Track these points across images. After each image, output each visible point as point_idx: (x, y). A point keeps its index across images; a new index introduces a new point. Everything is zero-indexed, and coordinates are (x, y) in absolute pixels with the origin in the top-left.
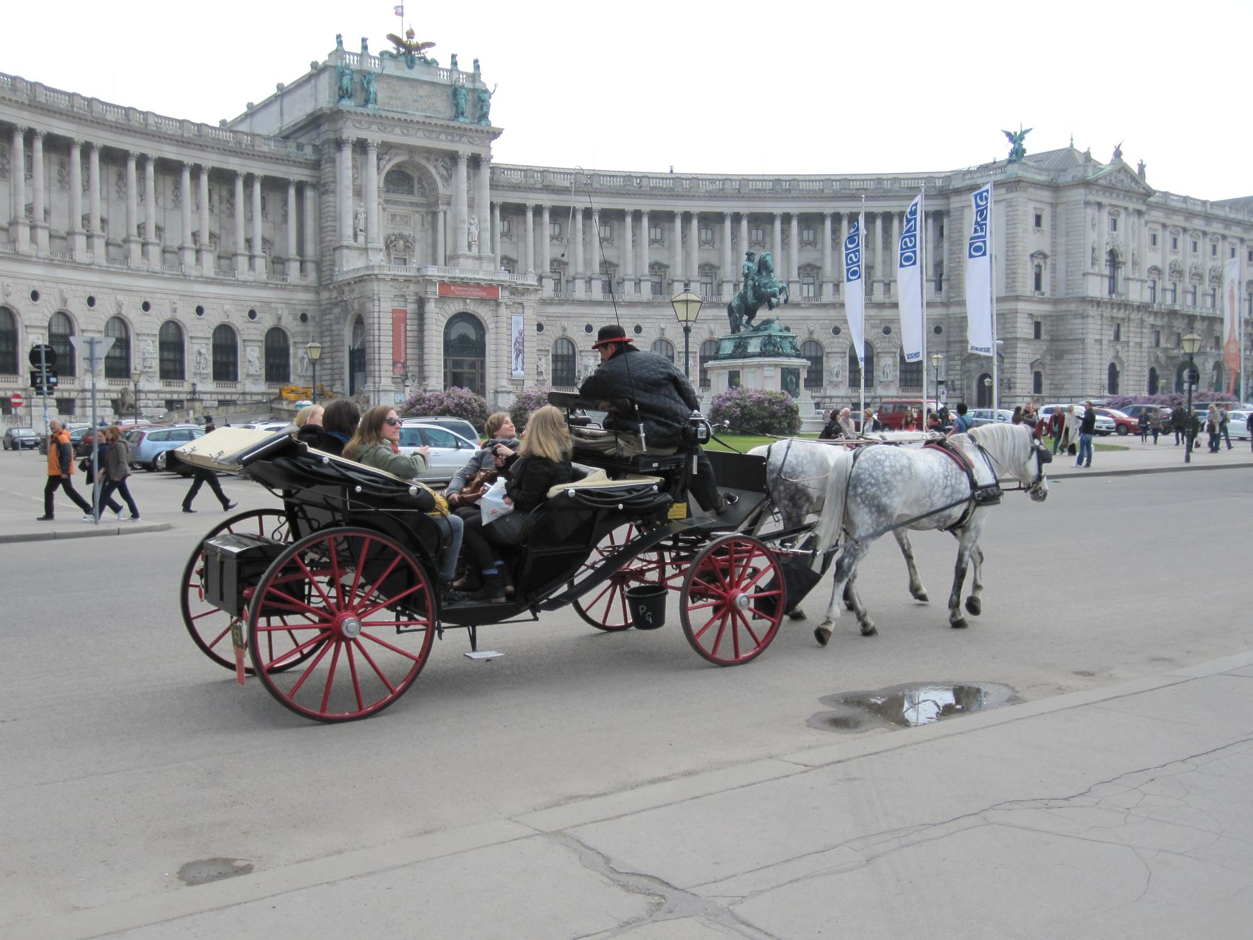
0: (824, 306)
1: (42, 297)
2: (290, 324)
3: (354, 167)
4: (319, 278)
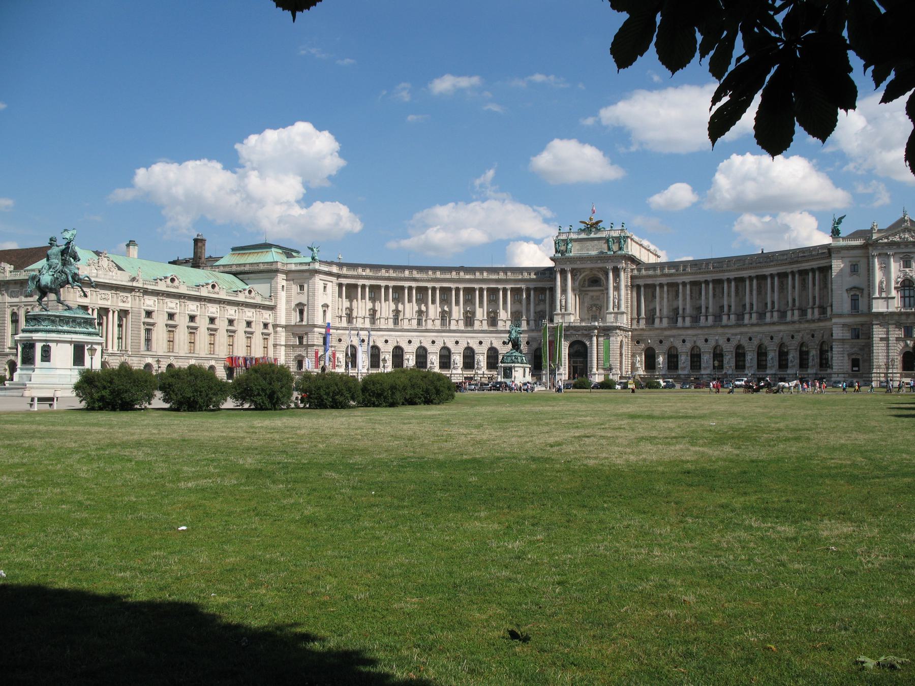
0: (786, 323)
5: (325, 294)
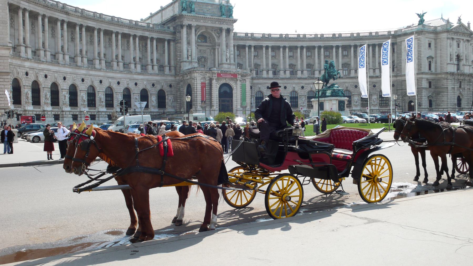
1: (85, 80)
2: (166, 89)
3: (187, 34)
4: (175, 72)
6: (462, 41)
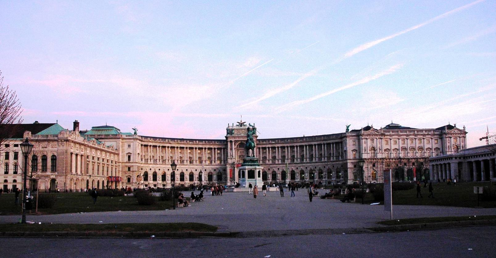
5: (137, 147)
6: (375, 139)
